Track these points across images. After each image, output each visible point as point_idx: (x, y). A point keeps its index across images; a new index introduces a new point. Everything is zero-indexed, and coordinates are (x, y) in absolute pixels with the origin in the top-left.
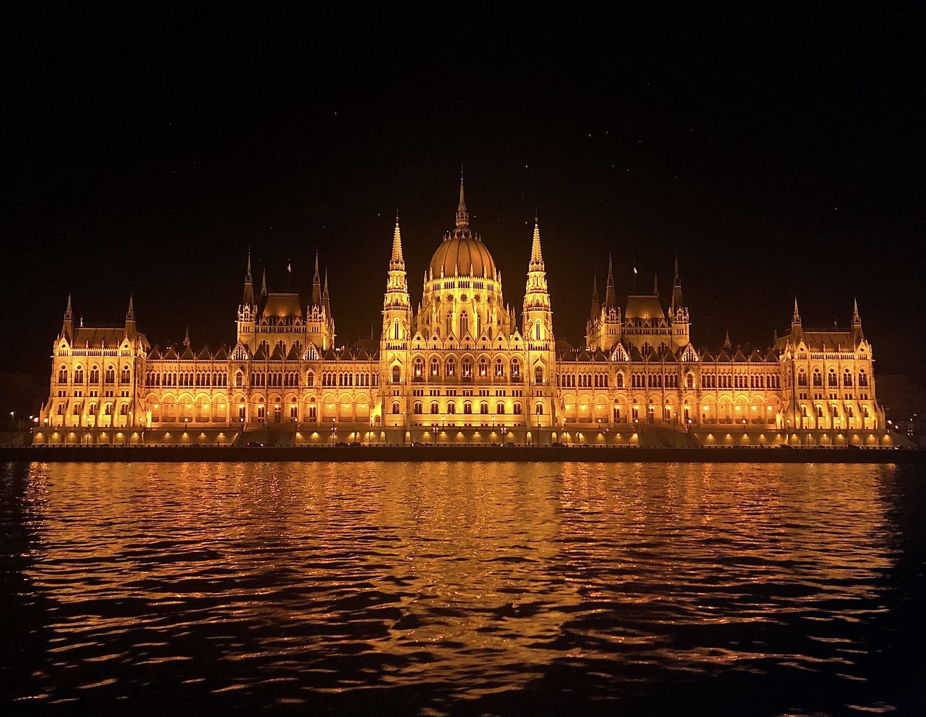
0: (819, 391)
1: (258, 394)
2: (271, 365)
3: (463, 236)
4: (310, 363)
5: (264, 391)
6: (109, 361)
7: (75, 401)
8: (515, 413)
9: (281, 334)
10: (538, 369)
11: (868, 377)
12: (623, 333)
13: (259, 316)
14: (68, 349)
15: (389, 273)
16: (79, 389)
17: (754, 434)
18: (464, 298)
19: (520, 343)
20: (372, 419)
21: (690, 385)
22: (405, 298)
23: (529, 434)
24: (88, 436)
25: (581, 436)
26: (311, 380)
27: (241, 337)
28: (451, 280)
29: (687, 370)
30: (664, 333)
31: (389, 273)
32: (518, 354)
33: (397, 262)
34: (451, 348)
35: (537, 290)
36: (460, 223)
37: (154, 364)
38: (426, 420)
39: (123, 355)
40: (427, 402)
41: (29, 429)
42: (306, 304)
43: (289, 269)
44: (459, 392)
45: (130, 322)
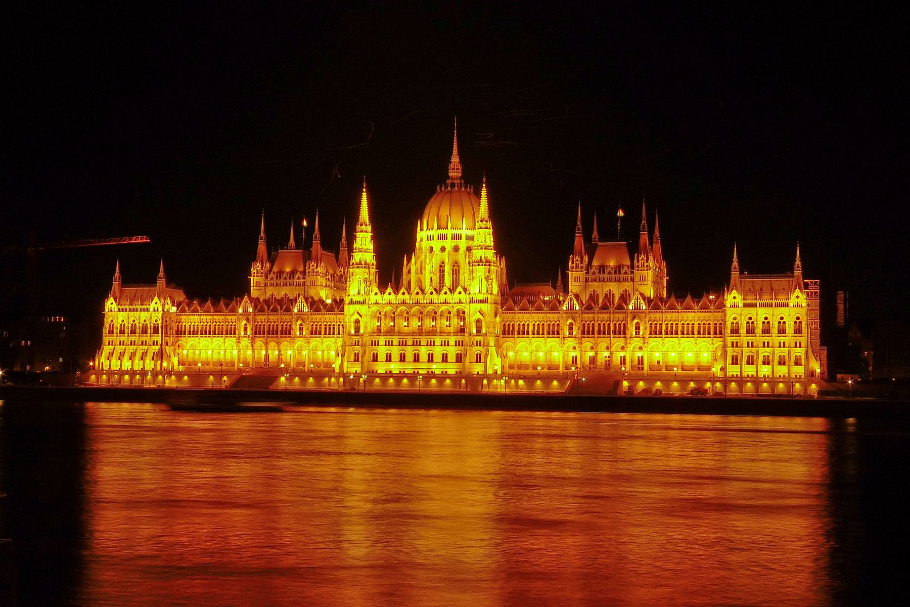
0: (750, 339)
1: (259, 342)
2: (270, 317)
3: (449, 189)
4: (301, 314)
6: (144, 315)
8: (457, 361)
9: (285, 288)
10: (478, 321)
11: (804, 325)
12: (587, 281)
13: (270, 271)
14: (115, 307)
15: (357, 234)
18: (443, 249)
19: (463, 295)
20: (336, 366)
23: (463, 381)
24: (127, 377)
25: (521, 382)
26: (301, 329)
27: (254, 292)
28: (430, 233)
29: (634, 318)
30: (626, 280)
31: (357, 234)
32: (459, 306)
33: (361, 225)
34: (404, 303)
35: (480, 247)
37: (183, 317)
39: (154, 310)
40: (382, 351)
41: (86, 370)
42: (307, 257)
43: (305, 223)
44: (410, 342)
45: (161, 283)
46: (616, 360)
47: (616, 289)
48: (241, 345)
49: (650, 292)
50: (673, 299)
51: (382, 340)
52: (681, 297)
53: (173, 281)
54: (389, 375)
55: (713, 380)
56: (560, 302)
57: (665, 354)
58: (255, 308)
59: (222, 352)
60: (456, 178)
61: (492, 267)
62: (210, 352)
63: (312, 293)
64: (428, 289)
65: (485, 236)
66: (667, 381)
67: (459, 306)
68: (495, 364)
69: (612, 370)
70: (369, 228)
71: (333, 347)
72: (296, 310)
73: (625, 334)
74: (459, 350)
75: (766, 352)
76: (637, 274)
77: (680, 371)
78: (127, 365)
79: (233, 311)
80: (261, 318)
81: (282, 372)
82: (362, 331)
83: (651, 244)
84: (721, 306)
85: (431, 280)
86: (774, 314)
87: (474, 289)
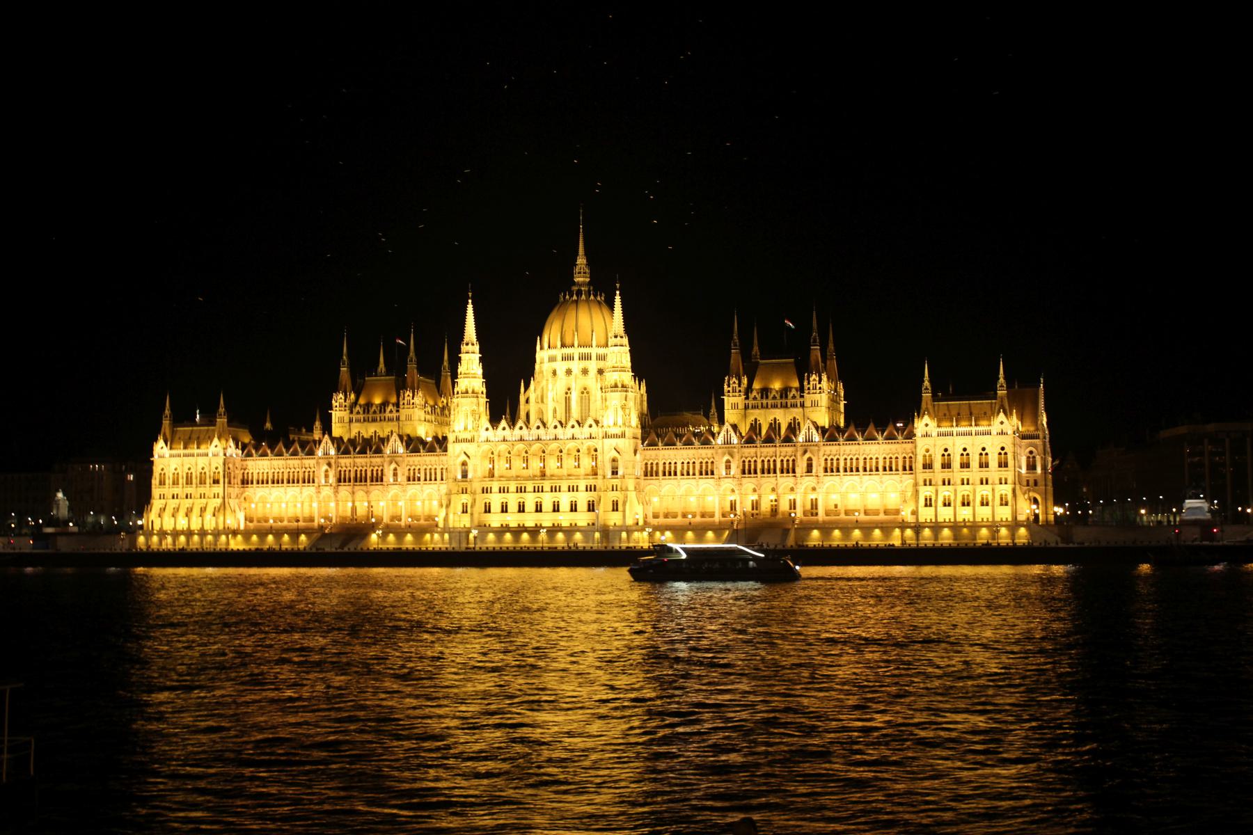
0: (946, 474)
1: (344, 490)
2: (358, 460)
3: (575, 297)
5: (349, 489)
6: (202, 462)
7: (172, 503)
10: (614, 460)
11: (1010, 456)
12: (746, 407)
13: (355, 403)
16: (176, 490)
17: (867, 529)
18: (569, 372)
21: (809, 469)
22: (478, 384)
23: (597, 535)
24: (182, 538)
26: (395, 475)
27: (337, 430)
28: (552, 352)
29: (805, 452)
30: (794, 406)
32: (591, 443)
34: (521, 440)
35: (614, 369)
36: (578, 279)
38: (495, 520)
40: (496, 500)
41: (133, 532)
42: (401, 386)
44: (530, 488)
45: (222, 421)
46: (784, 506)
47: (783, 418)
48: (321, 496)
49: (824, 421)
50: (852, 429)
51: (495, 486)
52: (862, 427)
53: (236, 420)
54: (504, 529)
55: (903, 526)
56: (713, 435)
57: (844, 496)
58: (338, 449)
59: (299, 505)
60: (583, 284)
61: (630, 394)
62: (284, 505)
63: (408, 430)
64: (551, 422)
65: (621, 355)
66: (846, 529)
67: (591, 443)
68: (635, 512)
69: (780, 516)
70: (477, 348)
71: (436, 496)
72: (387, 450)
73: (794, 472)
74: (591, 496)
75: (964, 490)
76: (808, 398)
77: (862, 517)
78: (182, 524)
79: (311, 453)
80: (346, 462)
81: (373, 527)
82: (470, 476)
83: (824, 359)
84: (911, 436)
85: (555, 411)
86: (974, 444)
87: (608, 420)
